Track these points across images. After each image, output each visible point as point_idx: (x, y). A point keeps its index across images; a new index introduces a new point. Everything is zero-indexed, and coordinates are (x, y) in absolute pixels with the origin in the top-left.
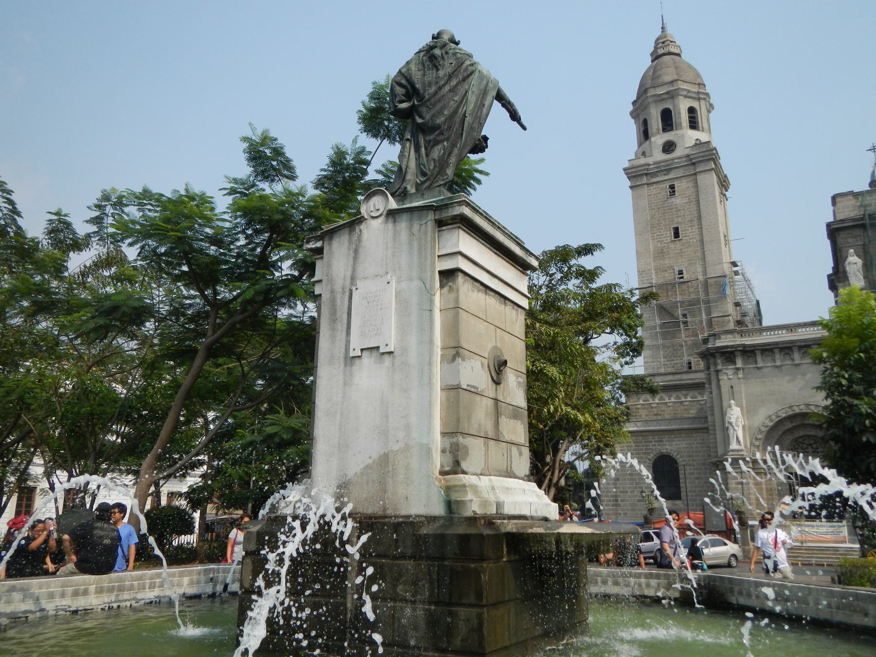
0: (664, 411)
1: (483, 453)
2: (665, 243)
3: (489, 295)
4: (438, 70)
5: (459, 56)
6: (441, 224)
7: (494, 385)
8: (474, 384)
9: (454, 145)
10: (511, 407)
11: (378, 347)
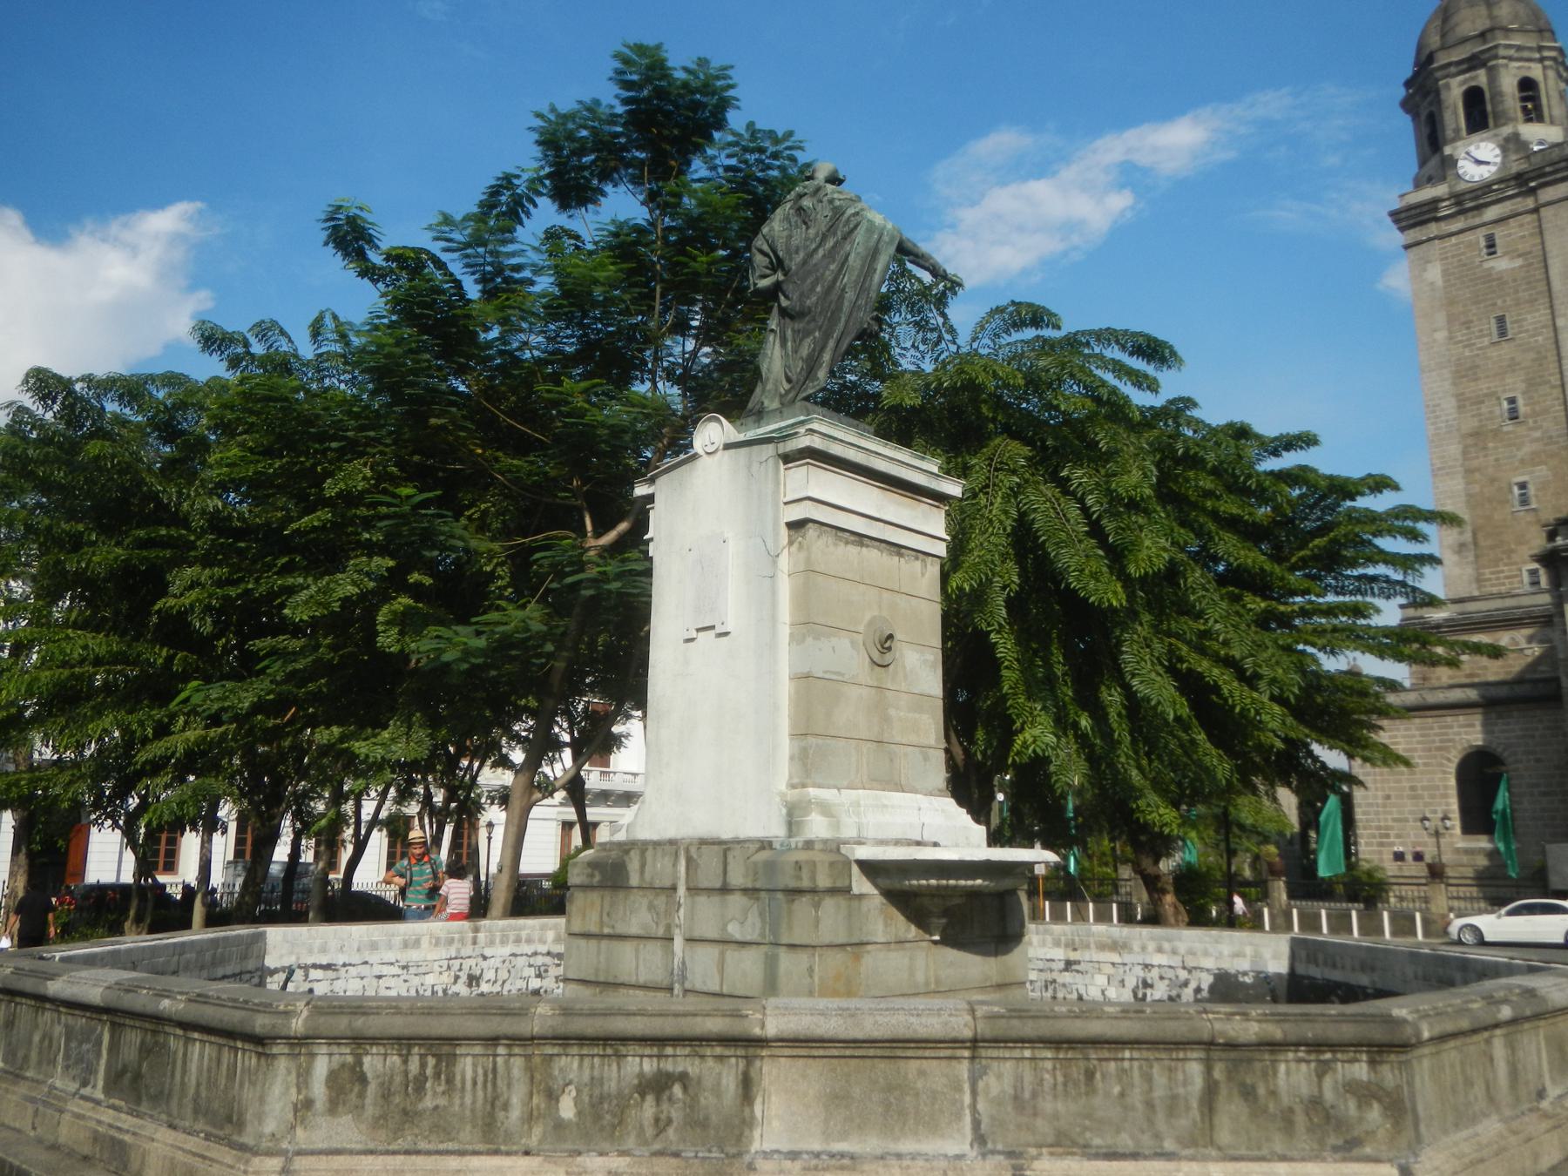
0: (1485, 668)
2: (1480, 349)
3: (867, 546)
4: (807, 228)
5: (837, 203)
6: (787, 458)
9: (827, 336)
11: (713, 627)
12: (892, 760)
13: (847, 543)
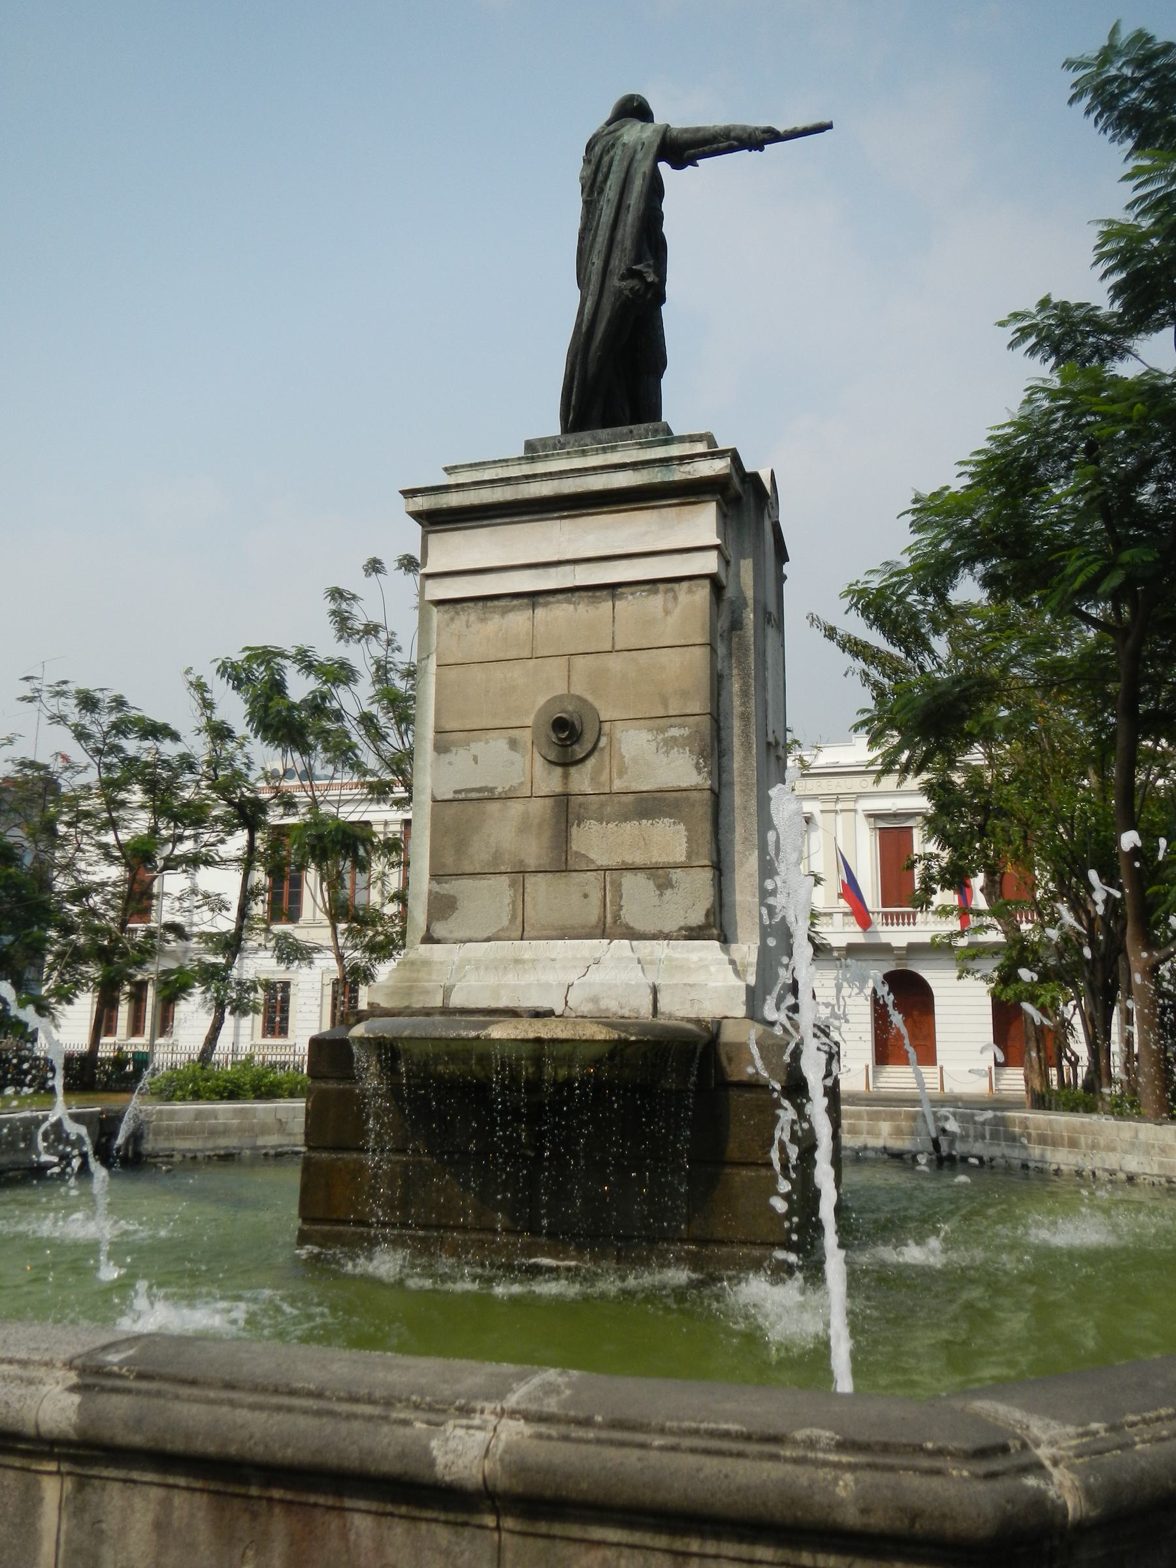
1: (507, 900)
3: (546, 605)
7: (559, 771)
8: (478, 785)
10: (631, 797)
12: (586, 896)
13: (505, 612)
